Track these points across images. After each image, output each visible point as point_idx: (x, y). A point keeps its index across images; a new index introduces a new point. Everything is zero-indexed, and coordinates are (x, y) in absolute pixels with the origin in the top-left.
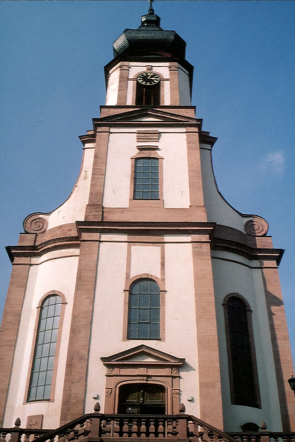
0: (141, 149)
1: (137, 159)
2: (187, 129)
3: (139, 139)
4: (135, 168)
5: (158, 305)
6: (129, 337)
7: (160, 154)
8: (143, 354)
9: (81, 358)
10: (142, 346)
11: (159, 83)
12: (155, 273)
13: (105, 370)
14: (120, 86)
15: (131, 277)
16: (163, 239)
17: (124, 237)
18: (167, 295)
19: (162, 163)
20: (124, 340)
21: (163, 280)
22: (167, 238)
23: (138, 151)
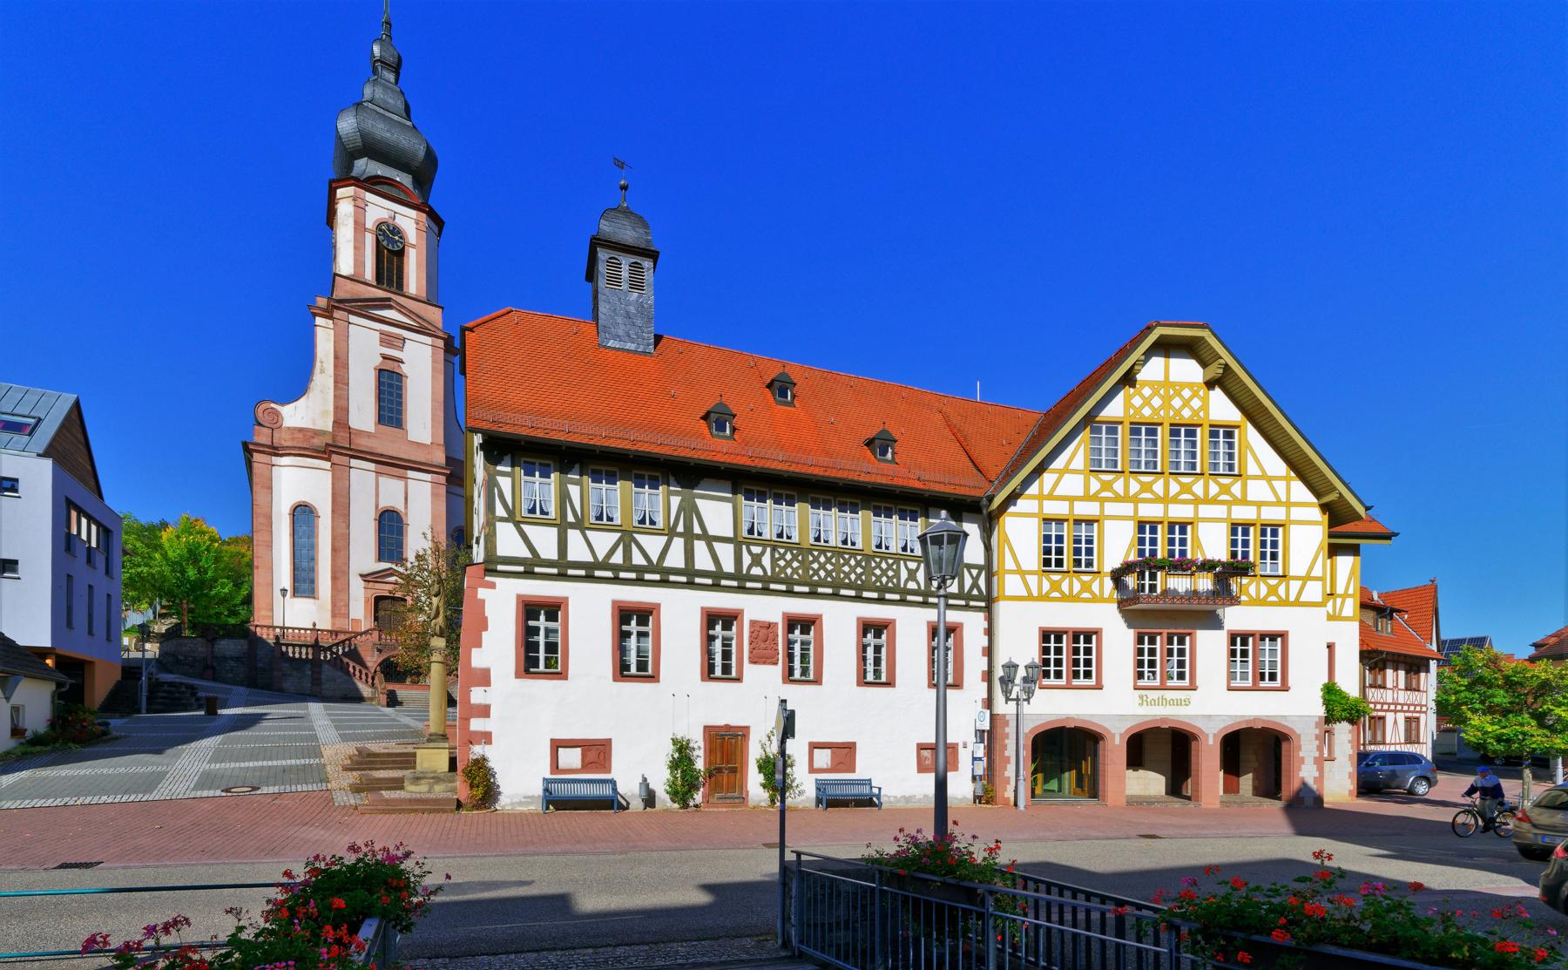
0: (385, 357)
1: (380, 370)
2: (433, 341)
3: (383, 342)
4: (380, 384)
5: (402, 535)
6: (380, 558)
7: (405, 369)
8: (392, 575)
9: (343, 572)
10: (391, 568)
11: (404, 248)
12: (400, 507)
13: (362, 584)
14: (356, 239)
15: (380, 507)
16: (406, 474)
17: (372, 466)
18: (409, 528)
19: (406, 383)
20: (376, 562)
21: (406, 514)
22: (411, 474)
23: (382, 359)
